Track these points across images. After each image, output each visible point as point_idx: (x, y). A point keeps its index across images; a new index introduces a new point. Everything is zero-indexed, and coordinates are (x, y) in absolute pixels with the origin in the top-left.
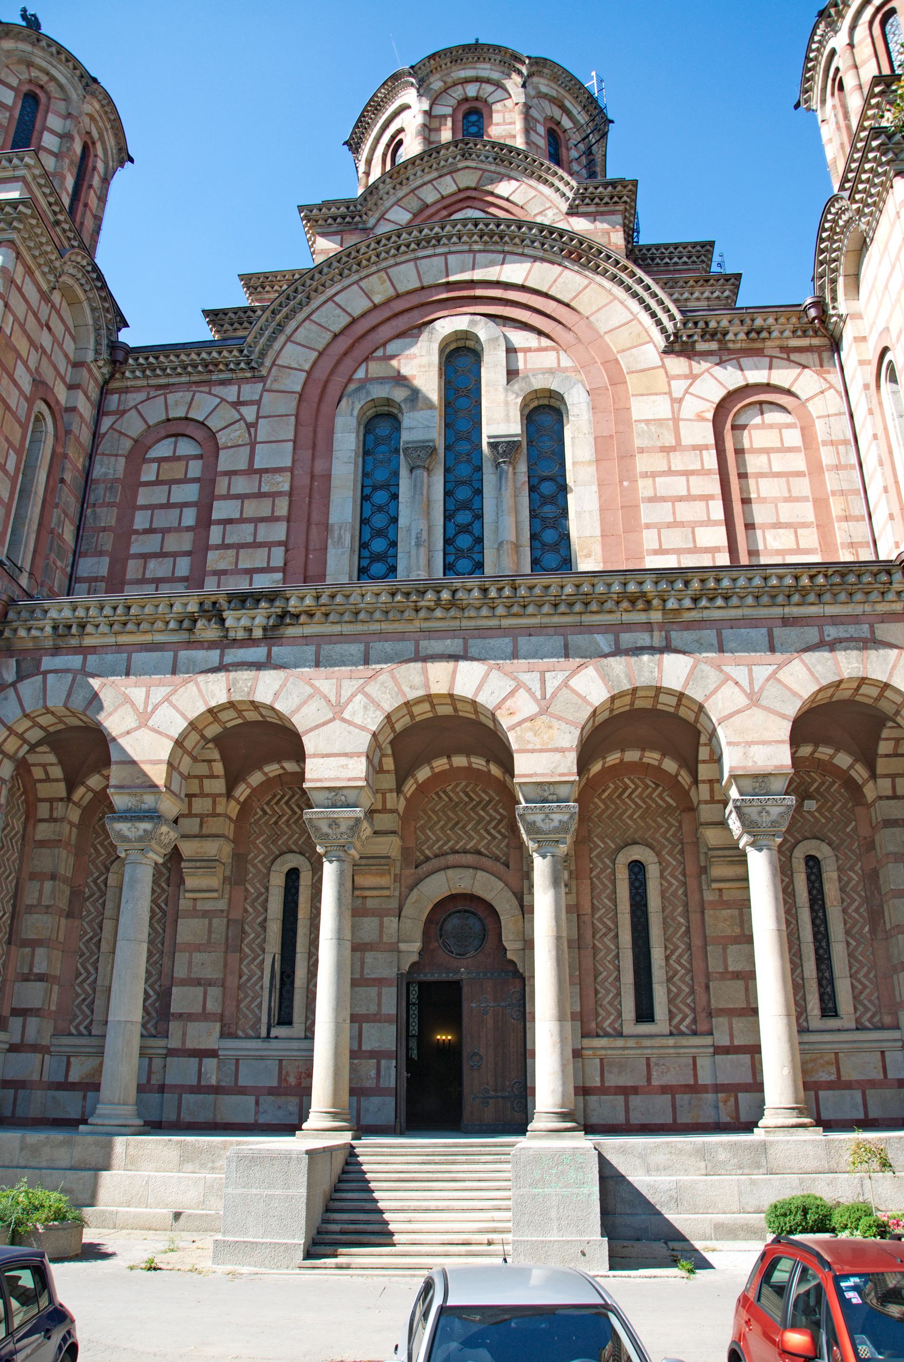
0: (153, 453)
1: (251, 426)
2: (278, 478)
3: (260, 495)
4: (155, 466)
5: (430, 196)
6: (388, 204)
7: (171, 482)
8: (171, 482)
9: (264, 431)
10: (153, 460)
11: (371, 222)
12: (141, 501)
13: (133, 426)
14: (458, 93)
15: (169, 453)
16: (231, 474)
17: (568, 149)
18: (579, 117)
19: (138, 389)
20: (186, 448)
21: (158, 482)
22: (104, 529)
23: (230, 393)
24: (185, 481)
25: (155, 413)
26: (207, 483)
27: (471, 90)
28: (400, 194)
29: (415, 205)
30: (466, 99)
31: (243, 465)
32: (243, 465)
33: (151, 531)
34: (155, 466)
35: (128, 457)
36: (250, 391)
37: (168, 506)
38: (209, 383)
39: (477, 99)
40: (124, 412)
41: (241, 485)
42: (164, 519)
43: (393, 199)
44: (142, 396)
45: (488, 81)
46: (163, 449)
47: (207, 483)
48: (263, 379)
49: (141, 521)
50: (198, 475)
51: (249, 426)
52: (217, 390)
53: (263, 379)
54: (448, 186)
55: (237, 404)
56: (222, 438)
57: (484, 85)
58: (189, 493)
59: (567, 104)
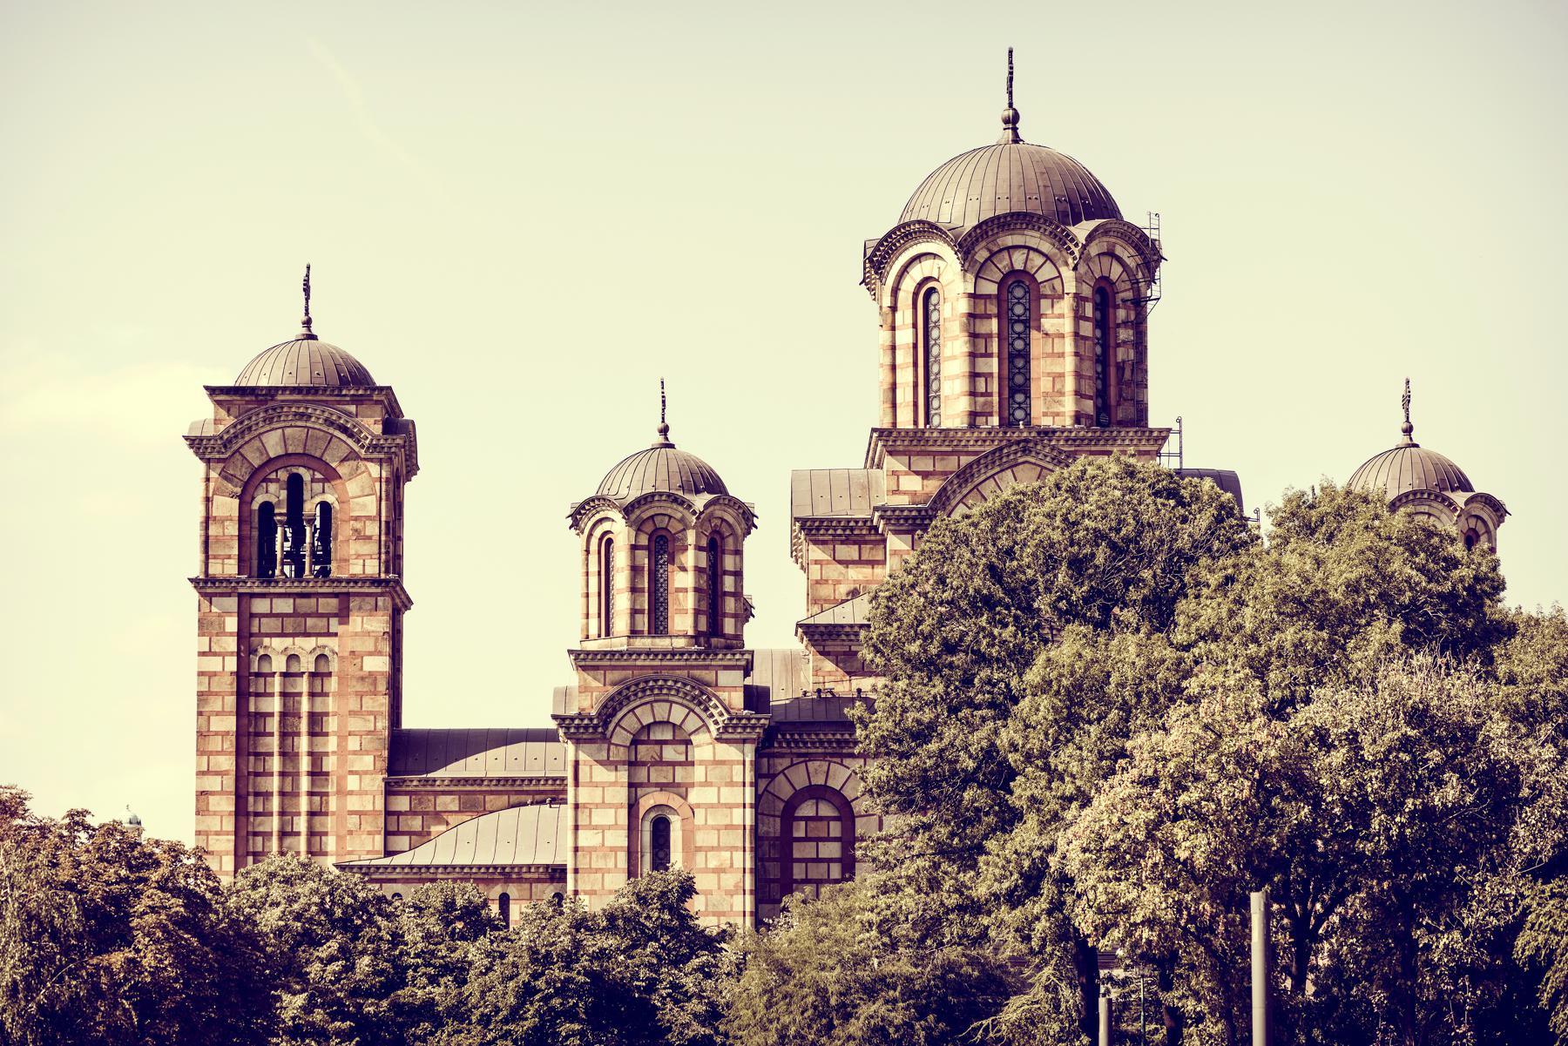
4: (803, 823)
6: (954, 503)
8: (818, 840)
10: (802, 818)
12: (796, 855)
13: (786, 792)
14: (1003, 263)
15: (812, 814)
17: (1117, 307)
18: (1128, 261)
19: (782, 756)
20: (826, 810)
21: (806, 839)
22: (774, 881)
24: (828, 839)
27: (1018, 260)
28: (965, 492)
30: (1013, 272)
34: (803, 823)
35: (782, 817)
37: (818, 860)
39: (1024, 272)
43: (959, 497)
44: (786, 762)
45: (1036, 250)
46: (807, 809)
50: (838, 835)
52: (847, 762)
57: (1032, 254)
58: (832, 850)
59: (1119, 251)
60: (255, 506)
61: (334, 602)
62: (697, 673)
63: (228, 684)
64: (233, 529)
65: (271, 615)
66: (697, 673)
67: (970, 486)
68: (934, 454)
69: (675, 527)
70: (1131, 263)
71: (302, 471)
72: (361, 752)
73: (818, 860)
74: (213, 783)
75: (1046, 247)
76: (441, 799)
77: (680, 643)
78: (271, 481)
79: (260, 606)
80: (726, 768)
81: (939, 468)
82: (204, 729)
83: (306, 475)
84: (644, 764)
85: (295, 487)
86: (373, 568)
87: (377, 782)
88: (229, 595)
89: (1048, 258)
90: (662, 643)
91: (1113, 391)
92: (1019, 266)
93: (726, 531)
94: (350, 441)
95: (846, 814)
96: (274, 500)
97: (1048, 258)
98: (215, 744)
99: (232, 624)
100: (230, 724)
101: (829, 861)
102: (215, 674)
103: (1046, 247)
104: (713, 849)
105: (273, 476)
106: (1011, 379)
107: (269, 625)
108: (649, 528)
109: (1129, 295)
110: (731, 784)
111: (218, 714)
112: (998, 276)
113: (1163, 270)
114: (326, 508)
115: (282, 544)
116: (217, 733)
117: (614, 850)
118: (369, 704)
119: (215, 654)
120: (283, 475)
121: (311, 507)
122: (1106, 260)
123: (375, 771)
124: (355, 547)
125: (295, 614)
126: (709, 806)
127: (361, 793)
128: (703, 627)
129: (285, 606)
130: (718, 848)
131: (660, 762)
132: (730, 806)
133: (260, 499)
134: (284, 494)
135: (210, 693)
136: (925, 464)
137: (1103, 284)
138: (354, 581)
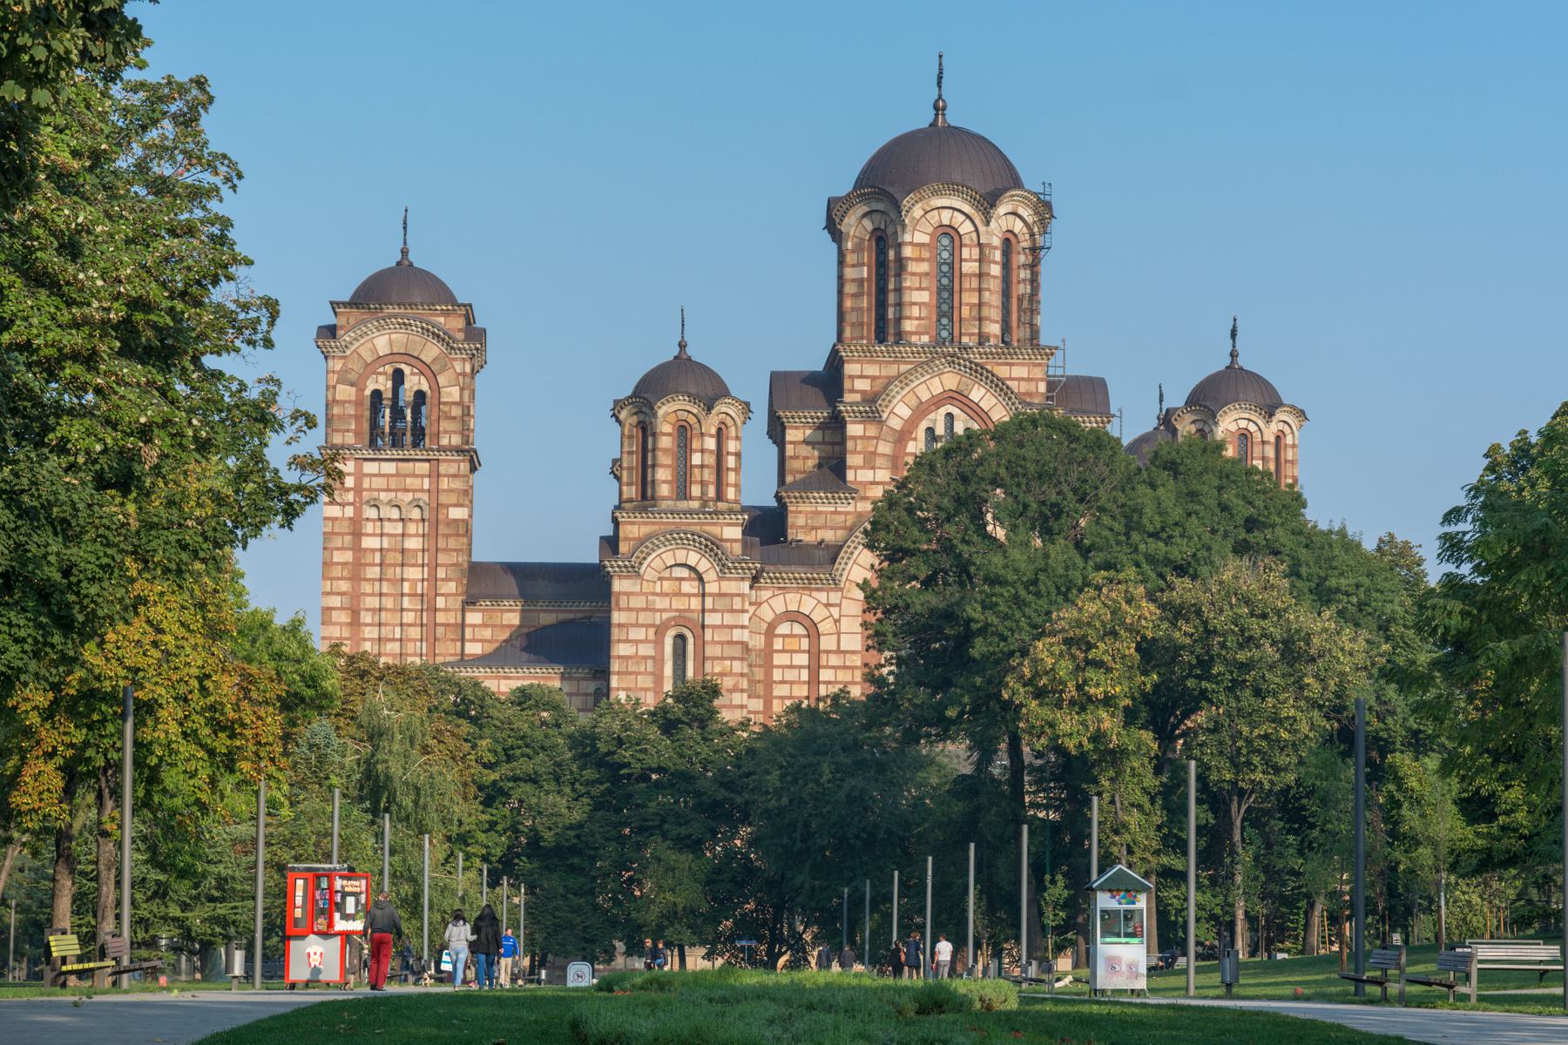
0: (778, 631)
1: (837, 621)
2: (854, 657)
3: (845, 667)
5: (925, 396)
7: (792, 652)
8: (792, 652)
9: (845, 625)
11: (885, 416)
12: (776, 662)
13: (769, 617)
14: (934, 217)
15: (788, 632)
16: (828, 652)
19: (766, 589)
20: (798, 629)
21: (783, 651)
23: (822, 596)
24: (799, 651)
25: (780, 608)
26: (815, 654)
27: (946, 217)
29: (914, 402)
31: (834, 648)
32: (834, 648)
33: (783, 682)
36: (835, 597)
37: (791, 667)
38: (810, 589)
40: (760, 604)
41: (834, 660)
42: (791, 675)
44: (769, 593)
46: (784, 628)
47: (815, 654)
48: (842, 590)
49: (777, 675)
51: (837, 621)
52: (815, 594)
53: (842, 590)
54: (936, 387)
55: (828, 605)
56: (821, 628)
58: (803, 659)
59: (1021, 211)
60: (368, 392)
61: (427, 465)
62: (707, 528)
63: (344, 527)
64: (351, 410)
65: (379, 475)
66: (707, 528)
67: (907, 389)
68: (880, 363)
69: (692, 420)
70: (1030, 220)
72: (447, 579)
73: (791, 667)
74: (336, 601)
75: (967, 208)
76: (506, 615)
77: (695, 505)
79: (370, 468)
80: (728, 600)
81: (884, 373)
83: (407, 370)
84: (667, 595)
85: (398, 377)
86: (456, 440)
87: (457, 603)
89: (968, 216)
90: (683, 505)
91: (1014, 317)
92: (946, 222)
93: (729, 421)
95: (813, 632)
96: (382, 388)
97: (968, 216)
98: (337, 571)
100: (348, 556)
101: (800, 667)
103: (967, 208)
104: (717, 658)
106: (939, 307)
107: (379, 483)
108: (672, 418)
109: (1026, 244)
110: (732, 611)
112: (930, 230)
113: (1054, 226)
114: (420, 396)
115: (386, 420)
117: (645, 658)
118: (452, 543)
120: (389, 369)
121: (407, 394)
122: (1011, 217)
123: (456, 595)
124: (444, 425)
125: (397, 475)
126: (714, 627)
127: (446, 610)
128: (712, 492)
129: (390, 468)
130: (723, 658)
131: (679, 594)
132: (732, 627)
133: (370, 387)
134: (390, 384)
136: (872, 370)
137: (1010, 236)
138: (441, 449)
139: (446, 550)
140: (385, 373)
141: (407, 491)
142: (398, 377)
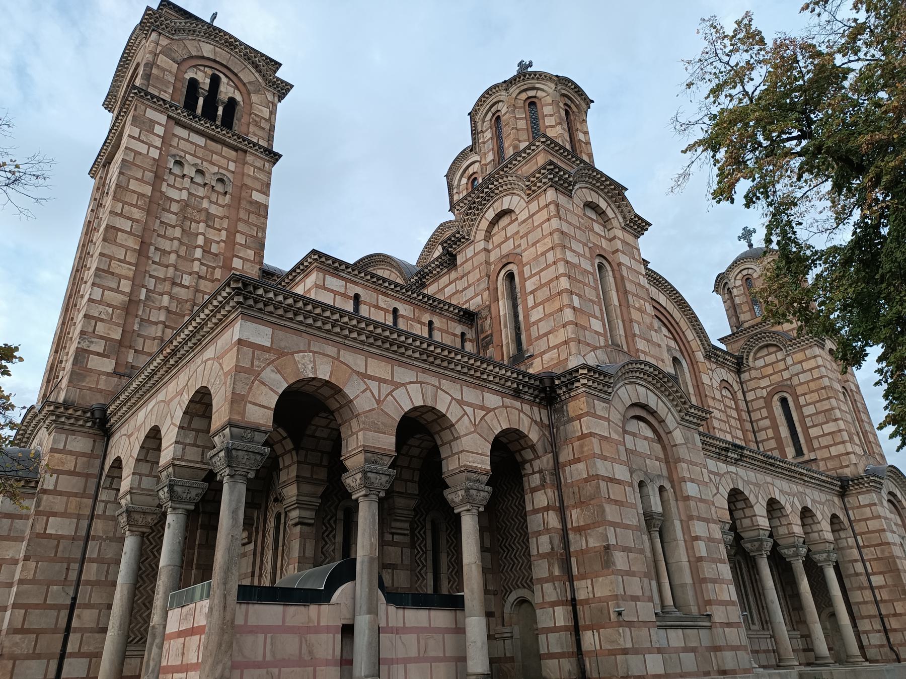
71: (221, 75)
72: (245, 246)
78: (200, 70)
82: (124, 184)
85: (215, 81)
88: (161, 112)
94: (257, 74)
99: (159, 130)
102: (140, 154)
105: (202, 68)
111: (137, 179)
116: (134, 192)
119: (143, 142)
120: (210, 72)
125: (205, 148)
135: (133, 164)
139: (247, 222)
140: (205, 73)
141: (214, 164)
142: (215, 81)
